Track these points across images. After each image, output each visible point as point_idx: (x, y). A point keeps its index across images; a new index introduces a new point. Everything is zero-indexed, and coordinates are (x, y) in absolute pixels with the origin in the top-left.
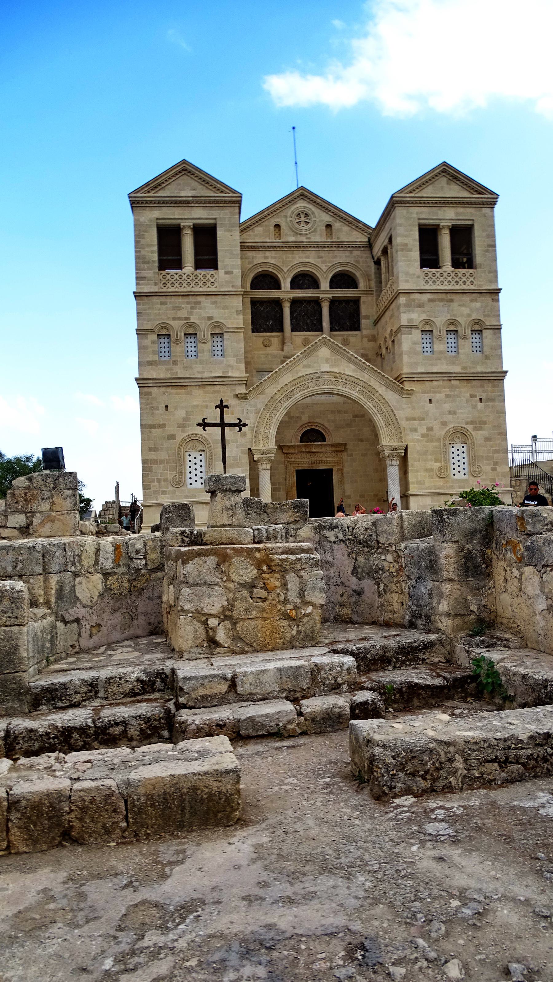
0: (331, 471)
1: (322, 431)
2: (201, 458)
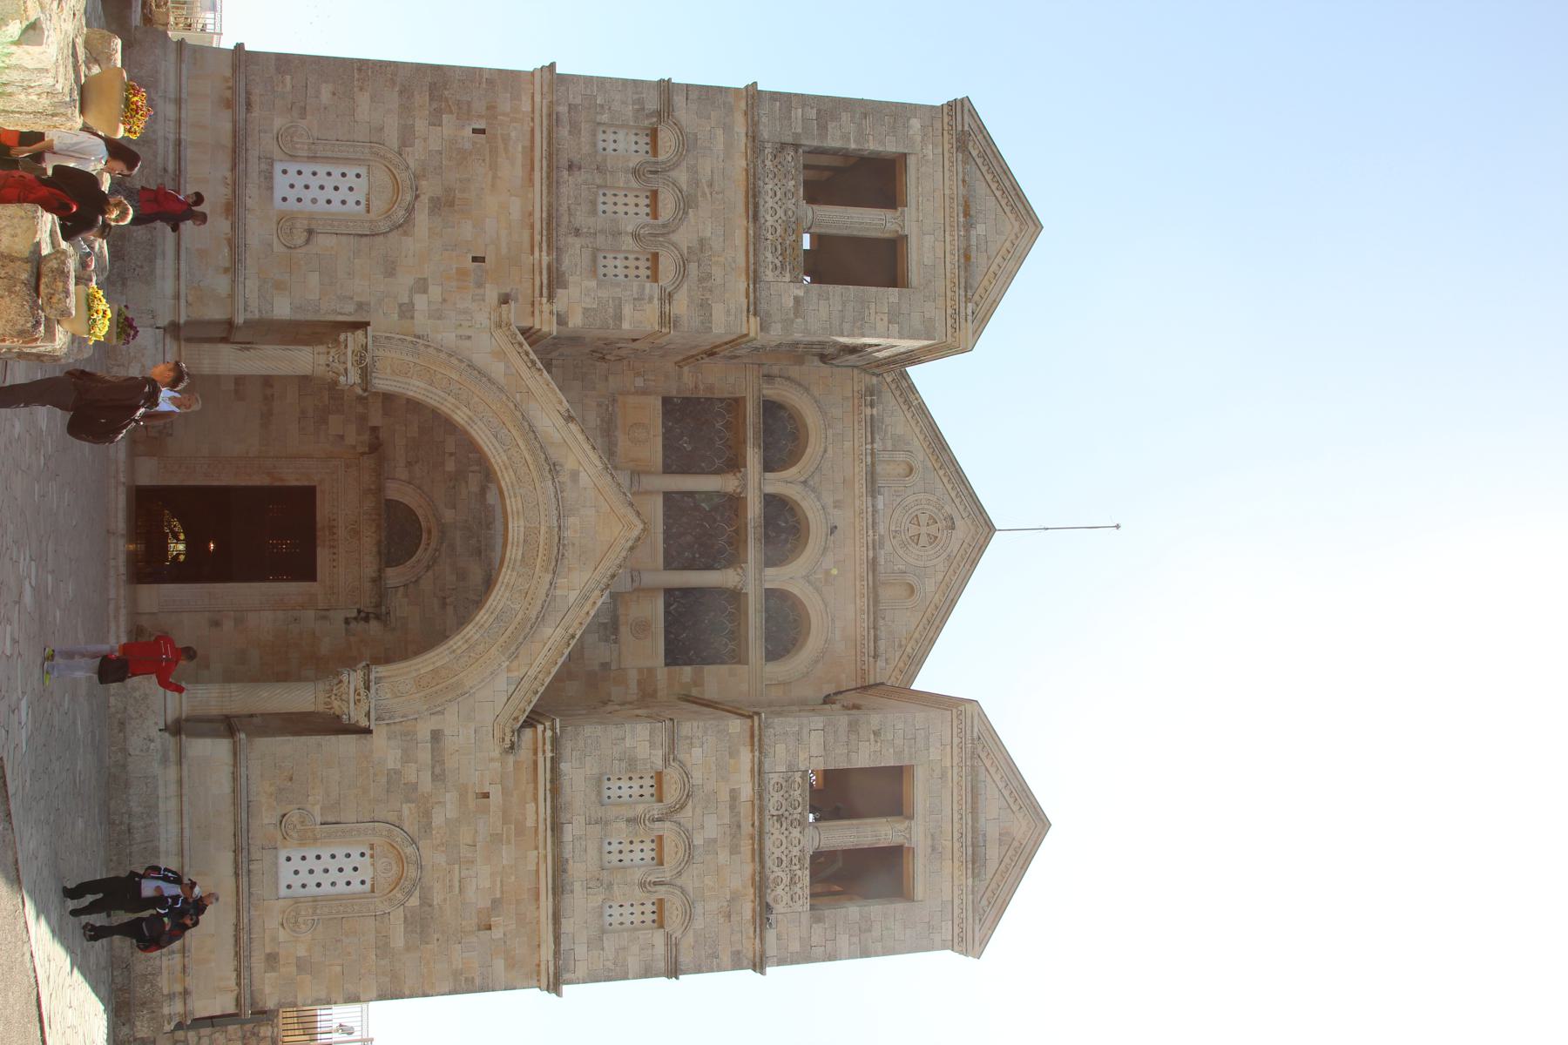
0: (312, 576)
1: (414, 559)
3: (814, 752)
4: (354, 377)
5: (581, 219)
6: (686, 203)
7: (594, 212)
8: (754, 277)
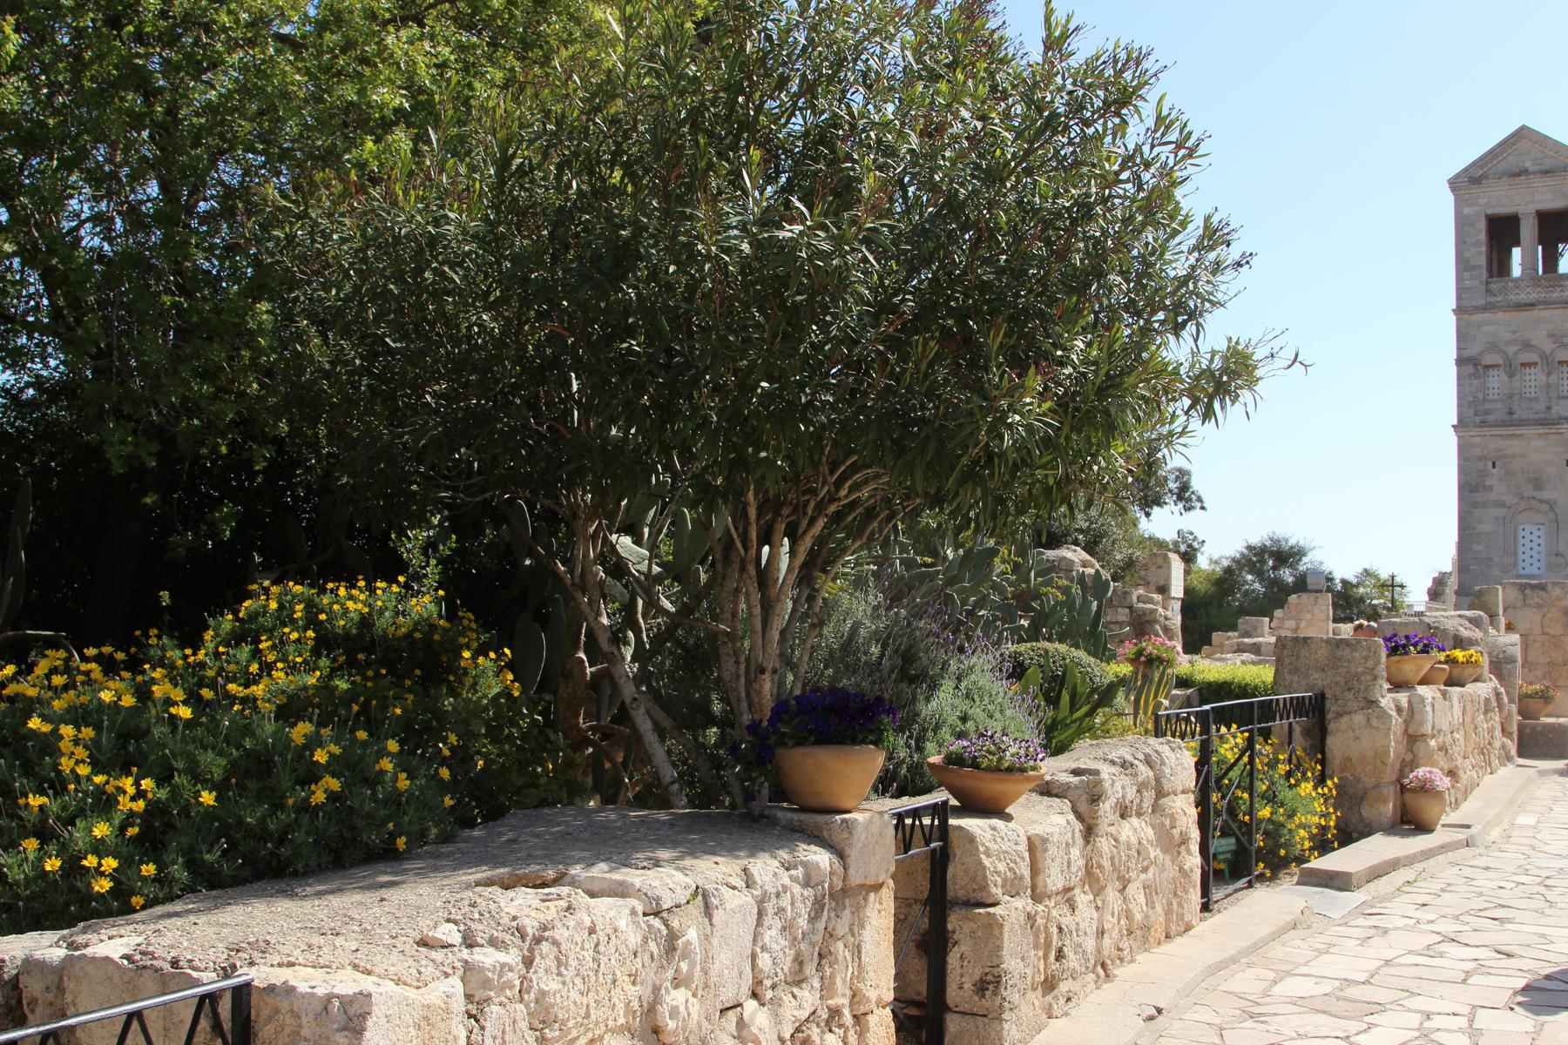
2: (1539, 533)
5: (1541, 406)
6: (1527, 345)
7: (1536, 399)
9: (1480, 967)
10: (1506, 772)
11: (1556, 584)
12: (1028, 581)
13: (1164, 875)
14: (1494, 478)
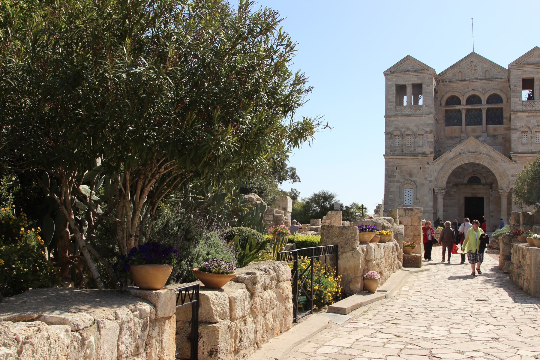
2: (411, 192)
3: (519, 100)
4: (443, 191)
5: (412, 149)
6: (408, 129)
7: (411, 147)
8: (422, 115)
9: (389, 341)
10: (399, 272)
11: (416, 208)
12: (237, 205)
13: (280, 310)
14: (397, 173)
